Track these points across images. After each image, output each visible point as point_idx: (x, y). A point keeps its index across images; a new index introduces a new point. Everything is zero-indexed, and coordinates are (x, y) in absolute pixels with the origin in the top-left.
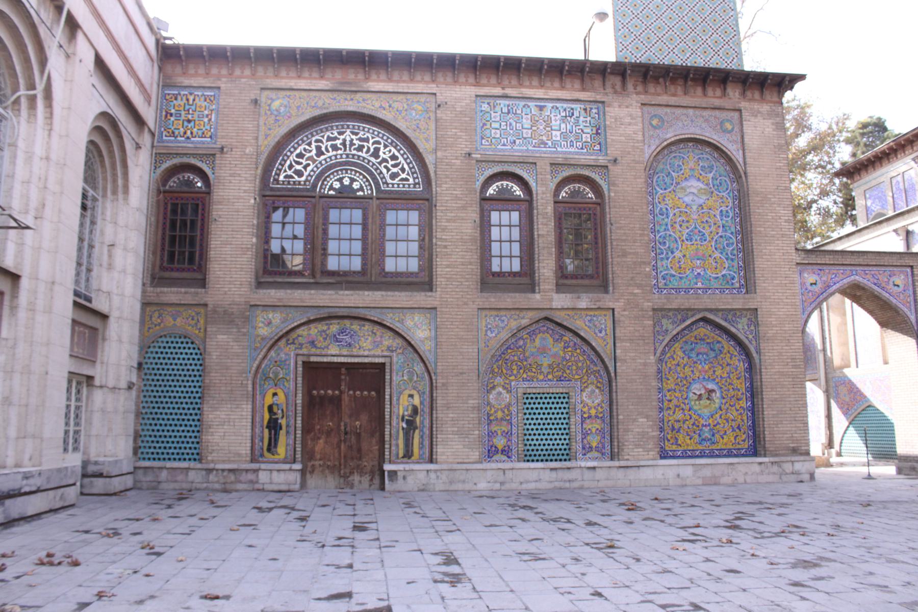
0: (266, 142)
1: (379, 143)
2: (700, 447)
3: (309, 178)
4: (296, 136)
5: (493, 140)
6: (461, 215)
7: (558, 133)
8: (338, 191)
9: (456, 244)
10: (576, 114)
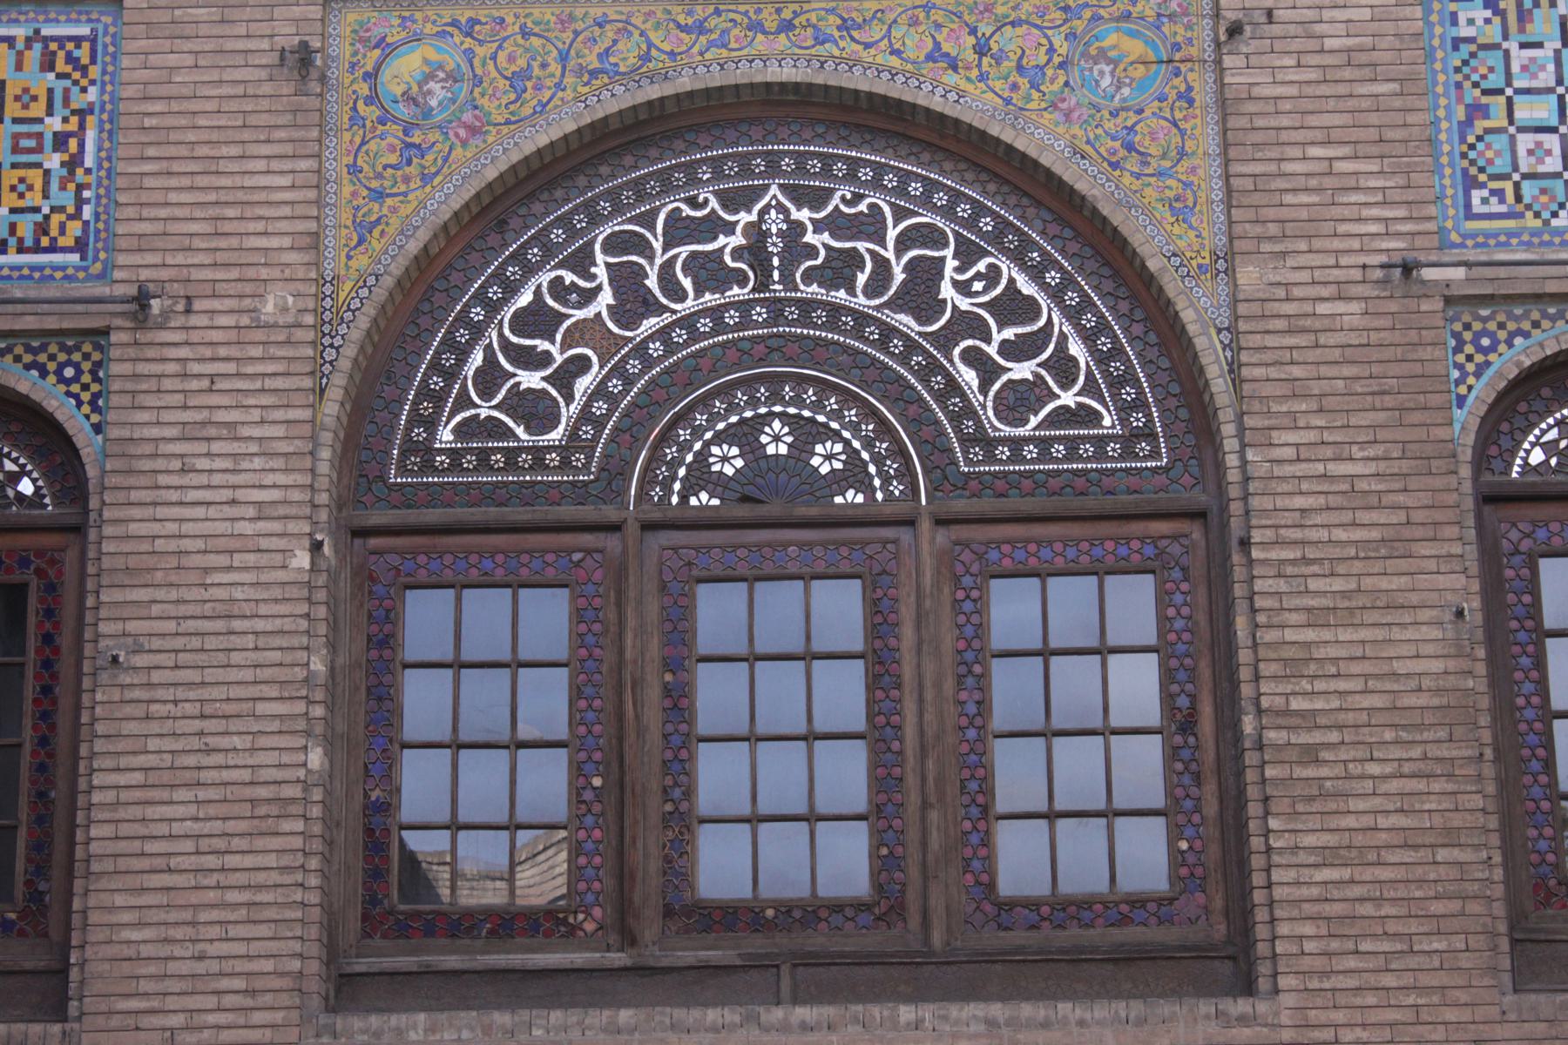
0: (361, 261)
1: (933, 237)
3: (587, 431)
4: (515, 223)
5: (1529, 189)
6: (1384, 583)
8: (740, 491)
9: (1366, 735)
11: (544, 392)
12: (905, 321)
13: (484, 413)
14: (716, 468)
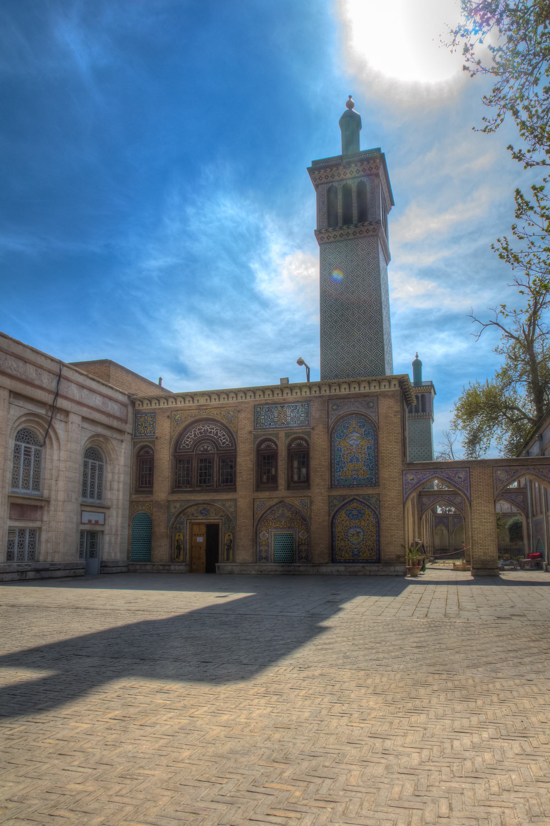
2: (352, 558)
7: (289, 418)
10: (298, 408)
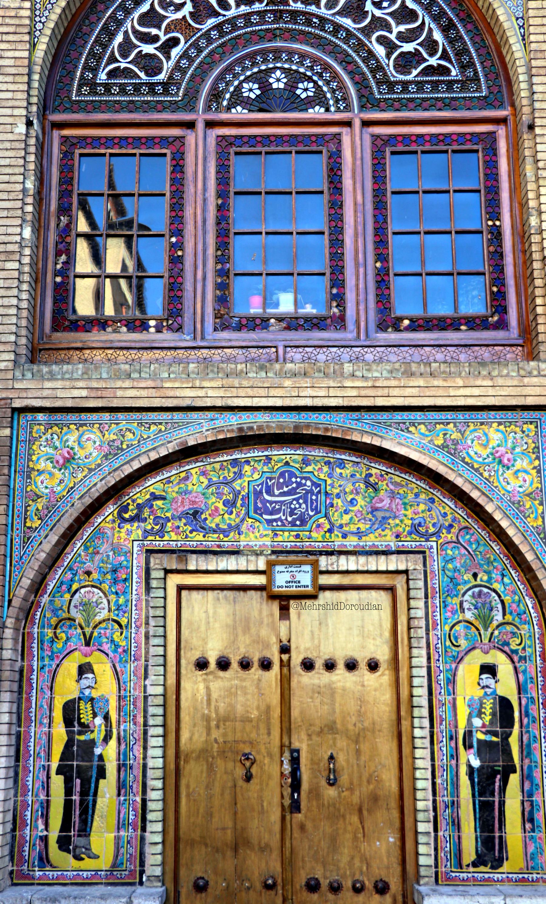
3: (177, 75)
11: (154, 55)
12: (347, 22)
13: (123, 66)
14: (245, 95)
